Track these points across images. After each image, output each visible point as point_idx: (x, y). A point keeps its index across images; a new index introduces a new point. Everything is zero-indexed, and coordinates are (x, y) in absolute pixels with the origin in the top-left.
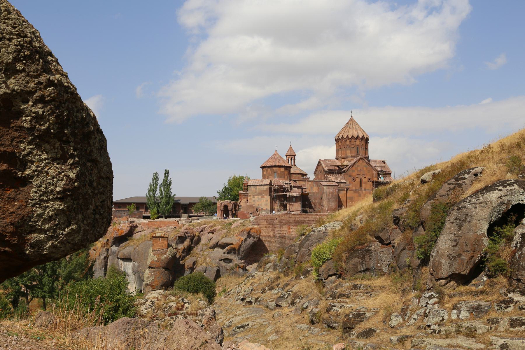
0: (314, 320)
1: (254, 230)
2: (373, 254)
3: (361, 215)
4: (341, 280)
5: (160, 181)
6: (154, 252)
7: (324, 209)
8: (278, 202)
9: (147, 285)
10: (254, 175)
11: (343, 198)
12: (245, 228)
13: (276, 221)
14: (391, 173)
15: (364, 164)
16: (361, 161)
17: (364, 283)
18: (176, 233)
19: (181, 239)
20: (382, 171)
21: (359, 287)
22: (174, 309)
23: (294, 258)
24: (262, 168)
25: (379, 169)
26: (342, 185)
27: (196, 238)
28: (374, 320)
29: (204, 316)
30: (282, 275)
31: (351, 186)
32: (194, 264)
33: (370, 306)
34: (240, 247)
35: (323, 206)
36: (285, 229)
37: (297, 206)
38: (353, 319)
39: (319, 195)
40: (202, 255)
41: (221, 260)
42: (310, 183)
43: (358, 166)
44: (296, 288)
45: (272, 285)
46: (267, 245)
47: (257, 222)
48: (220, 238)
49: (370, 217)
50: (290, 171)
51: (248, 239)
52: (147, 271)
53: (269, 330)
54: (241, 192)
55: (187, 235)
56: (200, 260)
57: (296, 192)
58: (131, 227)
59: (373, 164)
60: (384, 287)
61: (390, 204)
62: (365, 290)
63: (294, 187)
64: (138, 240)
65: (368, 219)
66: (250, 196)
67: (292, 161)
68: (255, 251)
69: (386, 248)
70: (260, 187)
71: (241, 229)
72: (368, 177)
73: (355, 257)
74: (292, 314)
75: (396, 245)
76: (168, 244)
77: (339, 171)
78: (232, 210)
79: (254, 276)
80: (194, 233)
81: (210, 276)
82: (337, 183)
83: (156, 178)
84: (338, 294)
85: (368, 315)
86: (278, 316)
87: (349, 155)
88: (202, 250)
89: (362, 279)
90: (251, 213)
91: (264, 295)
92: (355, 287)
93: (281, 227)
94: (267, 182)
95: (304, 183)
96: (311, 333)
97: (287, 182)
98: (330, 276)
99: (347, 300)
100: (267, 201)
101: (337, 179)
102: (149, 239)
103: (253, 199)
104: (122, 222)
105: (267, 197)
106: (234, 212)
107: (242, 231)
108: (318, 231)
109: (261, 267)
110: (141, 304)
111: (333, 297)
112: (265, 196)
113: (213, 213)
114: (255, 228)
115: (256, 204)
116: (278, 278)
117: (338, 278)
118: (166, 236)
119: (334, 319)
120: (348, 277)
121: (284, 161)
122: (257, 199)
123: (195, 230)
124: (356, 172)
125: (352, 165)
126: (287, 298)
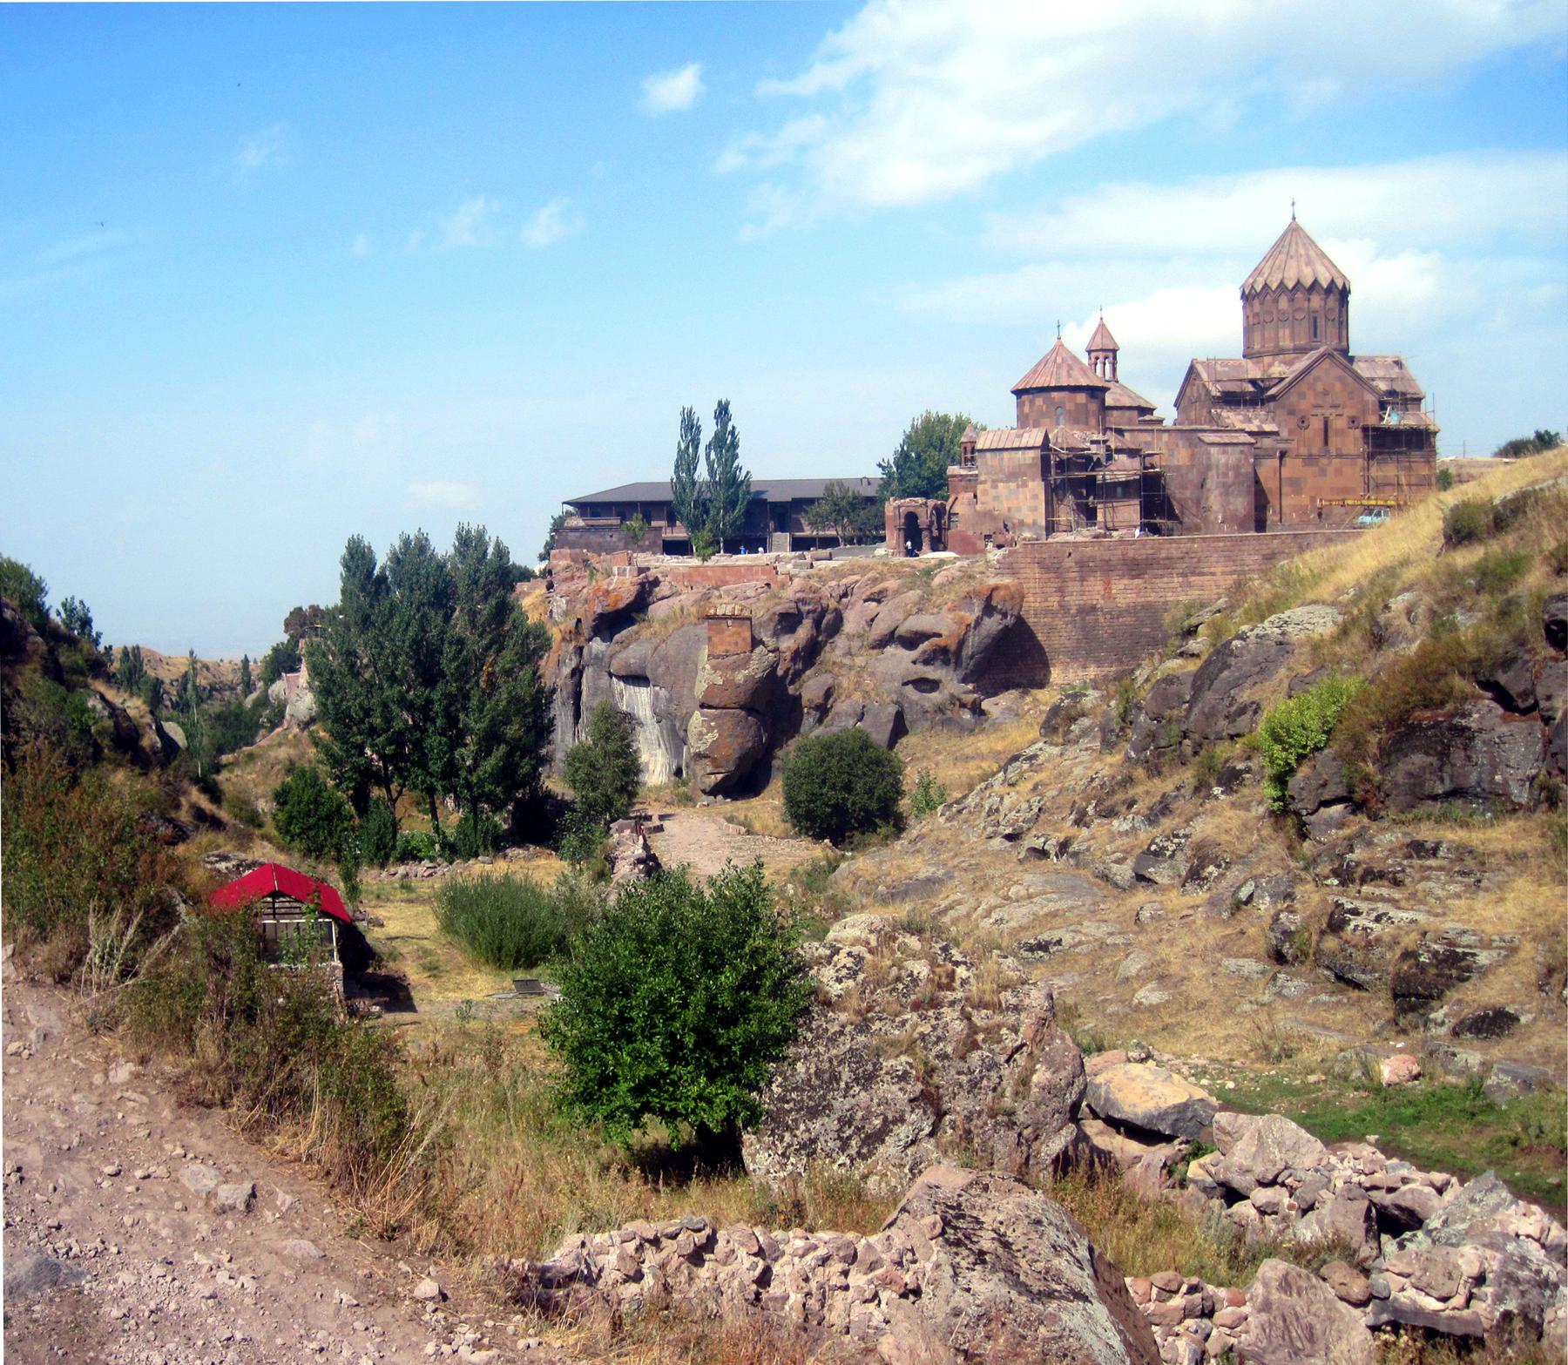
0: (1286, 948)
1: (1002, 593)
2: (1478, 743)
3: (1405, 590)
4: (1365, 820)
5: (707, 436)
6: (714, 661)
7: (1212, 518)
8: (1070, 498)
9: (700, 756)
10: (992, 414)
11: (1269, 484)
12: (974, 585)
13: (1069, 563)
14: (1419, 400)
15: (1337, 371)
16: (1326, 364)
17: (1452, 835)
18: (771, 603)
19: (788, 622)
20: (1392, 393)
21: (1434, 852)
22: (922, 992)
23: (1179, 721)
24: (1018, 393)
25: (1383, 386)
26: (1267, 442)
27: (828, 617)
28: (1507, 978)
29: (1023, 1015)
30: (1140, 773)
31: (1294, 445)
32: (828, 694)
33: (1488, 928)
34: (961, 643)
35: (1208, 509)
36: (1095, 586)
37: (1129, 511)
38: (1433, 971)
39: (1194, 476)
40: (851, 668)
41: (905, 684)
42: (1165, 436)
43: (1317, 379)
44: (1203, 828)
45: (1107, 803)
46: (1040, 637)
47: (1008, 567)
48: (901, 616)
49: (1440, 602)
50: (1103, 401)
51: (987, 620)
52: (697, 718)
53: (1133, 966)
54: (953, 470)
55: (805, 608)
56: (845, 682)
57: (1123, 469)
58: (642, 584)
59: (1362, 369)
60: (1524, 856)
61: (1517, 566)
62: (1452, 861)
63: (1119, 451)
64: (665, 623)
65: (1436, 607)
66: (983, 482)
67: (1108, 367)
68: (1008, 657)
69: (1519, 725)
71: (964, 588)
72: (1349, 412)
73: (1415, 749)
74: (1199, 917)
75: (1559, 715)
76: (753, 638)
77: (1256, 396)
78: (929, 529)
79: (1035, 756)
80: (824, 602)
81: (880, 735)
82: (1251, 434)
83: (690, 427)
84: (1360, 871)
85: (1483, 958)
86: (1152, 917)
87: (1286, 343)
88: (849, 653)
89: (1438, 822)
90: (988, 537)
91: (1085, 832)
92: (1417, 849)
93: (1083, 579)
94: (1034, 437)
95: (1147, 437)
96: (1279, 994)
97: (1095, 438)
98: (1327, 803)
99: (1396, 894)
100: (1035, 497)
101: (1250, 421)
102: (694, 620)
103: (993, 492)
104: (615, 570)
105: (1037, 487)
106: (936, 533)
107: (968, 596)
108: (1258, 636)
109: (1055, 730)
110: (819, 961)
111: (1345, 876)
112: (1030, 484)
113: (869, 536)
114: (1006, 587)
115: (1002, 508)
116: (1129, 781)
117: (1354, 812)
118: (747, 614)
119: (1359, 956)
120: (1392, 813)
121: (1083, 370)
123: (825, 591)
124: (1311, 399)
126: (1172, 856)
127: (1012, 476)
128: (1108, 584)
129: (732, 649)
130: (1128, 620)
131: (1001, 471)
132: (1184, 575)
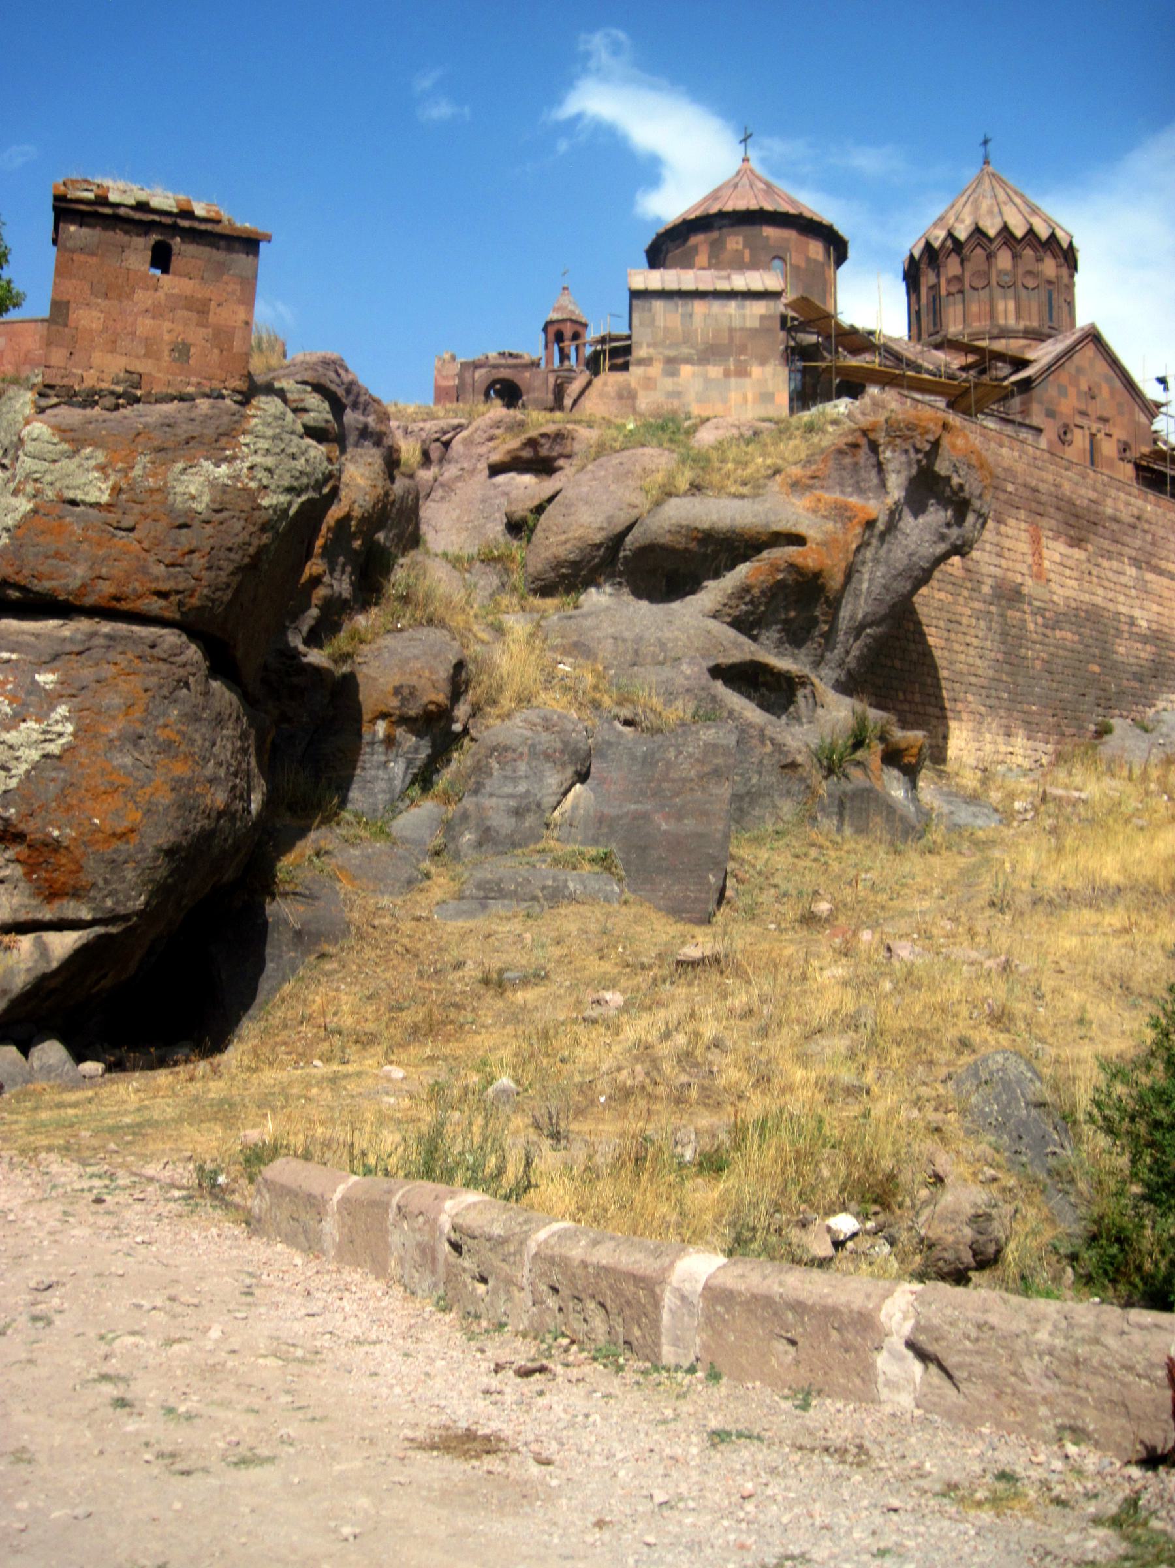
6: (71, 415)
16: (1090, 351)
43: (1079, 370)
48: (643, 502)
51: (908, 522)
66: (641, 362)
70: (716, 306)
72: (1119, 434)
100: (766, 397)
103: (668, 383)
112: (756, 371)
125: (1058, 359)
127: (710, 353)
129: (159, 373)
130: (1066, 635)
131: (687, 339)
132: (1135, 562)
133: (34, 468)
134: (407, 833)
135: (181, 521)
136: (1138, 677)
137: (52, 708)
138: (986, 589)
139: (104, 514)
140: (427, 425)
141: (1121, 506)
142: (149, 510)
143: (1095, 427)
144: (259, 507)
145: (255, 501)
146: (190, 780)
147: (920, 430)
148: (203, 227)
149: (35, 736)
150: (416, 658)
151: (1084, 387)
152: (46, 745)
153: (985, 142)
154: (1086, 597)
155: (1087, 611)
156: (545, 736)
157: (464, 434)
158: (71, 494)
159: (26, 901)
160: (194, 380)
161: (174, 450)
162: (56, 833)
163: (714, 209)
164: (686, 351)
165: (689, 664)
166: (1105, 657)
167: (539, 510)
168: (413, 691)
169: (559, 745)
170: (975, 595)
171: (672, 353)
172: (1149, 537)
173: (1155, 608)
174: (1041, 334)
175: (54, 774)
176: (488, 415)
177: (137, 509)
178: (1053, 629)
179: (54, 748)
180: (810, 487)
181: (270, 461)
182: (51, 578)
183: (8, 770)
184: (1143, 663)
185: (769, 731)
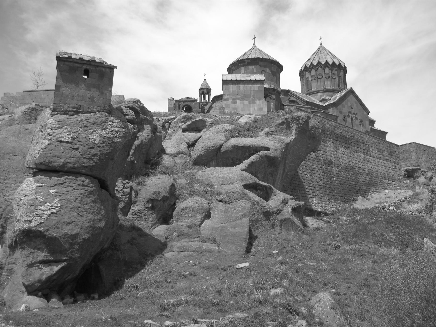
6: (61, 117)
52: (30, 184)
66: (226, 100)
72: (360, 118)
100: (261, 109)
103: (233, 106)
112: (258, 102)
122: (241, 106)
127: (244, 97)
128: (335, 148)
133: (50, 132)
134: (157, 233)
135: (91, 146)
136: (365, 185)
137: (54, 200)
138: (322, 161)
139: (69, 145)
140: (165, 118)
141: (359, 138)
142: (82, 143)
143: (353, 116)
144: (114, 142)
145: (112, 141)
146: (94, 219)
147: (301, 118)
148: (98, 65)
149: (49, 207)
150: (160, 183)
151: (349, 105)
152: (52, 210)
153: (321, 39)
154: (351, 163)
155: (350, 167)
156: (197, 205)
157: (175, 120)
158: (60, 139)
159: (46, 254)
160: (96, 107)
161: (90, 126)
162: (55, 235)
163: (246, 57)
164: (238, 96)
165: (238, 184)
166: (356, 180)
167: (196, 141)
168: (159, 193)
169: (201, 208)
170: (319, 163)
171: (234, 97)
172: (367, 146)
173: (370, 166)
174: (337, 90)
175: (54, 218)
176: (182, 115)
177: (79, 143)
178: (341, 172)
179: (54, 211)
180: (271, 134)
181: (117, 129)
182: (54, 163)
183: (41, 217)
184: (366, 181)
185: (260, 203)
